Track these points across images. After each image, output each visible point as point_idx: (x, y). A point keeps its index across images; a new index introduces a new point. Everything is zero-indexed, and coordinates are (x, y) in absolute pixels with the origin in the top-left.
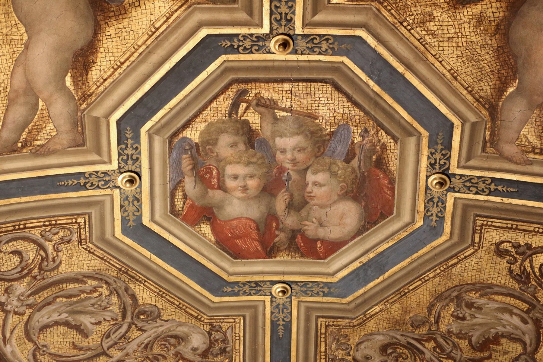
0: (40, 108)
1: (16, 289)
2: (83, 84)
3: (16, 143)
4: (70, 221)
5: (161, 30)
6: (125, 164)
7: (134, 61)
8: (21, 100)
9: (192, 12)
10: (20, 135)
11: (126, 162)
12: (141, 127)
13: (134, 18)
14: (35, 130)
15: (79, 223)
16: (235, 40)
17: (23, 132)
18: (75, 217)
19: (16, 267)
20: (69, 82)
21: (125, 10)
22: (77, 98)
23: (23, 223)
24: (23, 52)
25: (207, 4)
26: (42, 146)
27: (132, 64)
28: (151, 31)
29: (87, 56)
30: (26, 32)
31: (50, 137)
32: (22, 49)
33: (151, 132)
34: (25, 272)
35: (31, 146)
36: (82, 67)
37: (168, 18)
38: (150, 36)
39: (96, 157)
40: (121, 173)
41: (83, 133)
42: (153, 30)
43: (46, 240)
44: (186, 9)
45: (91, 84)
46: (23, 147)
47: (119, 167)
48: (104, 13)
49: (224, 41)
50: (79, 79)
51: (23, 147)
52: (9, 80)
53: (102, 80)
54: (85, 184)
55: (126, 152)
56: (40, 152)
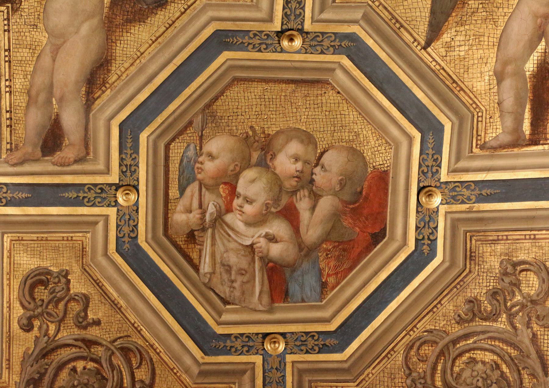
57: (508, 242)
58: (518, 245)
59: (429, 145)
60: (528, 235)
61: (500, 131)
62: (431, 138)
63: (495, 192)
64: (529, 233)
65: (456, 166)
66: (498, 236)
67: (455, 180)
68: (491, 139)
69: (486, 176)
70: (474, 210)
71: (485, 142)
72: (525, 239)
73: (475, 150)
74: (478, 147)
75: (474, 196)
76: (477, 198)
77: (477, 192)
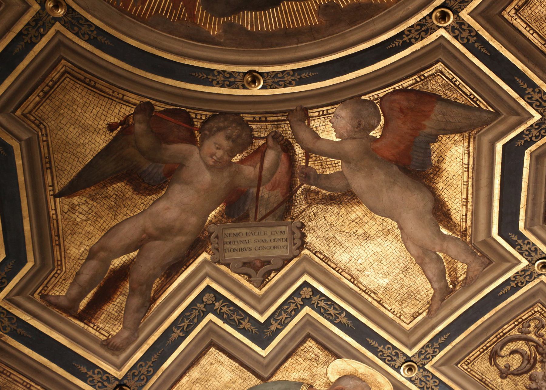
0: (442, 257)
1: (536, 375)
2: (455, 226)
3: (447, 286)
4: (530, 313)
5: (471, 163)
6: (531, 258)
7: (472, 193)
8: (427, 260)
9: (479, 139)
10: (446, 281)
11: (530, 255)
12: (518, 228)
13: (447, 169)
14: (452, 272)
15: (538, 311)
16: (524, 136)
17: (445, 278)
18: (531, 308)
19: (523, 361)
20: (445, 231)
21: (437, 167)
22: (459, 237)
23: (500, 331)
24: (401, 232)
25: (484, 128)
26: (465, 279)
27: (472, 195)
28: (466, 168)
29: (442, 209)
30: (393, 220)
31: (466, 270)
32: (399, 231)
33: (528, 226)
34: (532, 361)
35: (458, 283)
36: (444, 217)
37: (469, 153)
38: (468, 171)
39: (507, 265)
40: (534, 264)
41: (483, 255)
42: (466, 166)
43: (526, 334)
44: (474, 141)
45: (459, 223)
46: (455, 286)
47: (529, 261)
48: (427, 178)
49: (518, 142)
50: (449, 225)
51: (455, 286)
52: (408, 253)
53: (464, 217)
54: (517, 284)
55: (524, 249)
56: (467, 283)
57: (9, 379)
58: (13, 385)
59: (6, 269)
60: (26, 382)
61: (63, 293)
62: (11, 264)
63: (27, 335)
64: (28, 381)
65: (13, 297)
66: (5, 370)
67: (5, 307)
68: (53, 294)
69: (29, 320)
70: (2, 339)
71: (47, 294)
72: (22, 384)
73: (36, 295)
74: (40, 294)
75: (10, 329)
76: (11, 331)
77: (14, 327)
